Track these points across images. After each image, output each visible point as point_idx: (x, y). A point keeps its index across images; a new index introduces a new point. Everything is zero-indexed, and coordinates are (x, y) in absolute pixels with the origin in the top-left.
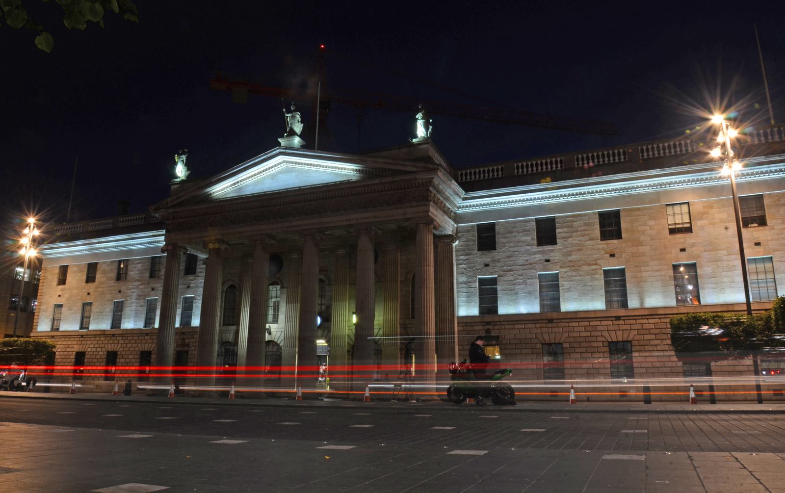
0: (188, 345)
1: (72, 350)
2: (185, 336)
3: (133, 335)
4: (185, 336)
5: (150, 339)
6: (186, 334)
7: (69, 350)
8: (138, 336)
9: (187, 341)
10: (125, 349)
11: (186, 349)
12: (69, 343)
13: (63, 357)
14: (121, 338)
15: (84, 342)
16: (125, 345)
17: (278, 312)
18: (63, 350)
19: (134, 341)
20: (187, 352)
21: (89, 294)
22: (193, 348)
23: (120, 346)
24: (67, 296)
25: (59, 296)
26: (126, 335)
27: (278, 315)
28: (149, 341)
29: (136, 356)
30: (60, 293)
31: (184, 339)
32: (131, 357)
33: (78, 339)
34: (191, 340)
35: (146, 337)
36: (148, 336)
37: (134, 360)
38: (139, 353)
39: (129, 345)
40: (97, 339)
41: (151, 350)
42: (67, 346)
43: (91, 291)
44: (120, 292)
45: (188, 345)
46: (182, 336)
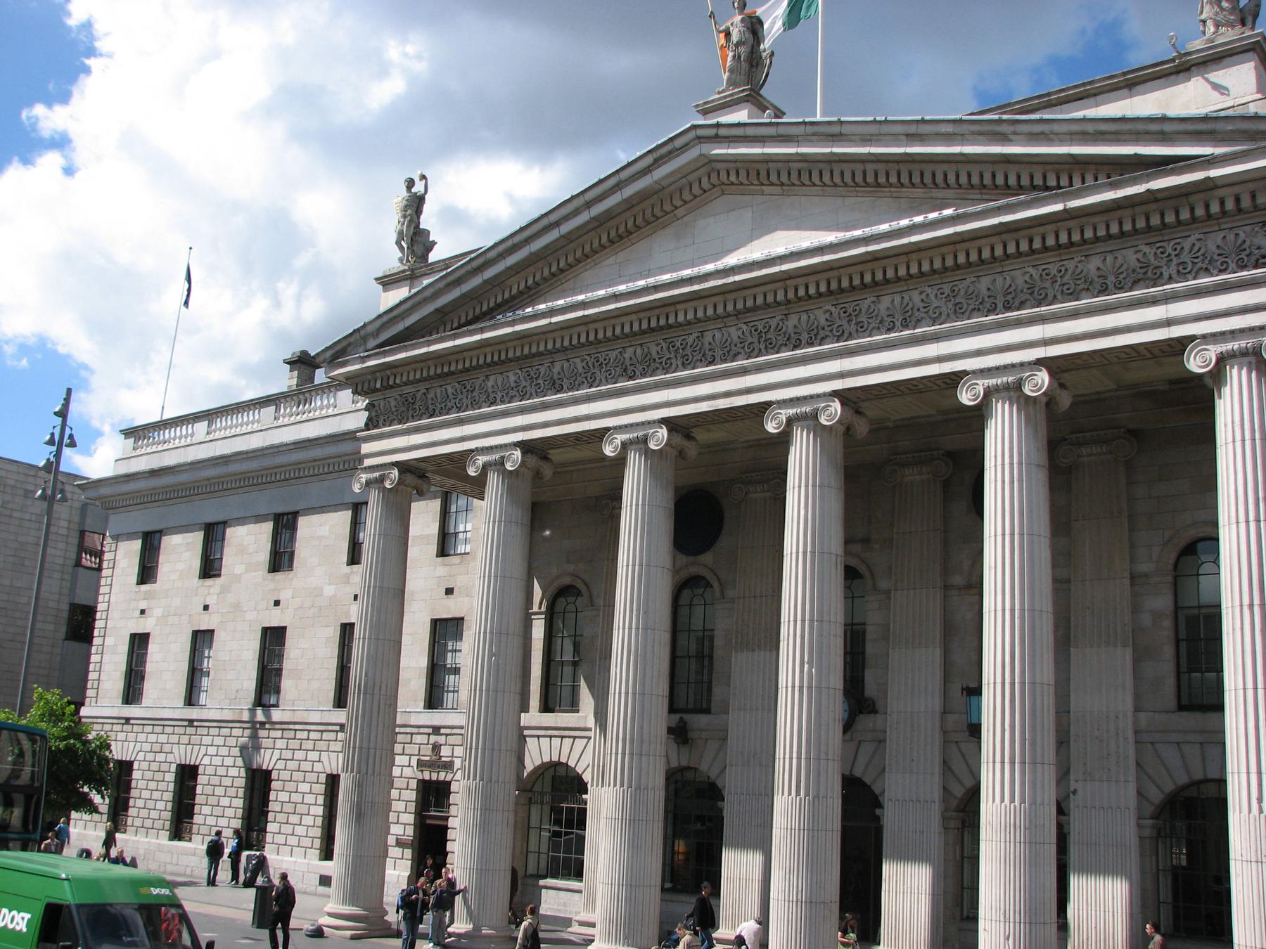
1: (170, 758)
2: (441, 739)
4: (441, 739)
7: (161, 757)
8: (322, 731)
9: (445, 751)
10: (292, 765)
12: (163, 738)
13: (149, 775)
14: (279, 734)
15: (195, 739)
16: (288, 754)
17: (710, 673)
18: (150, 757)
19: (309, 745)
21: (206, 608)
23: (277, 753)
24: (158, 612)
25: (143, 612)
26: (291, 727)
27: (710, 683)
30: (143, 605)
31: (436, 748)
32: (304, 787)
33: (182, 730)
38: (323, 778)
39: (300, 755)
40: (225, 731)
42: (157, 747)
43: (210, 601)
44: (277, 603)
45: (449, 766)
46: (433, 739)
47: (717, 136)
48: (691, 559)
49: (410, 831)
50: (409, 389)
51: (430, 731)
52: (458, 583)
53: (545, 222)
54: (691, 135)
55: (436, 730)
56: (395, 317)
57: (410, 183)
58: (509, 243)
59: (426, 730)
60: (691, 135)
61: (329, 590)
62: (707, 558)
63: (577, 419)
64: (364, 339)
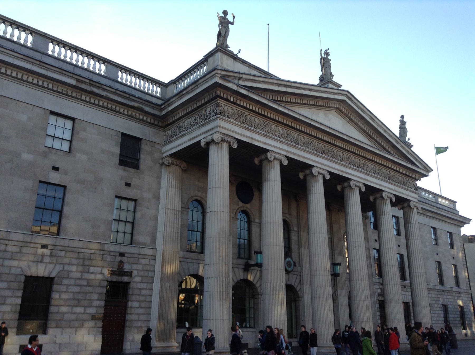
0: (130, 274)
2: (125, 259)
3: (7, 242)
4: (125, 259)
5: (51, 256)
6: (126, 255)
11: (125, 279)
20: (128, 283)
22: (138, 279)
28: (47, 259)
29: (14, 285)
34: (135, 267)
35: (40, 251)
36: (47, 248)
37: (9, 293)
38: (23, 279)
41: (52, 276)
45: (130, 274)
47: (351, 98)
48: (244, 205)
49: (102, 311)
50: (240, 110)
51: (118, 254)
52: (135, 181)
53: (310, 87)
54: (346, 93)
55: (122, 255)
56: (255, 80)
57: (225, 13)
58: (299, 85)
59: (115, 254)
60: (346, 93)
61: (27, 157)
62: (248, 206)
63: (304, 158)
64: (239, 79)
